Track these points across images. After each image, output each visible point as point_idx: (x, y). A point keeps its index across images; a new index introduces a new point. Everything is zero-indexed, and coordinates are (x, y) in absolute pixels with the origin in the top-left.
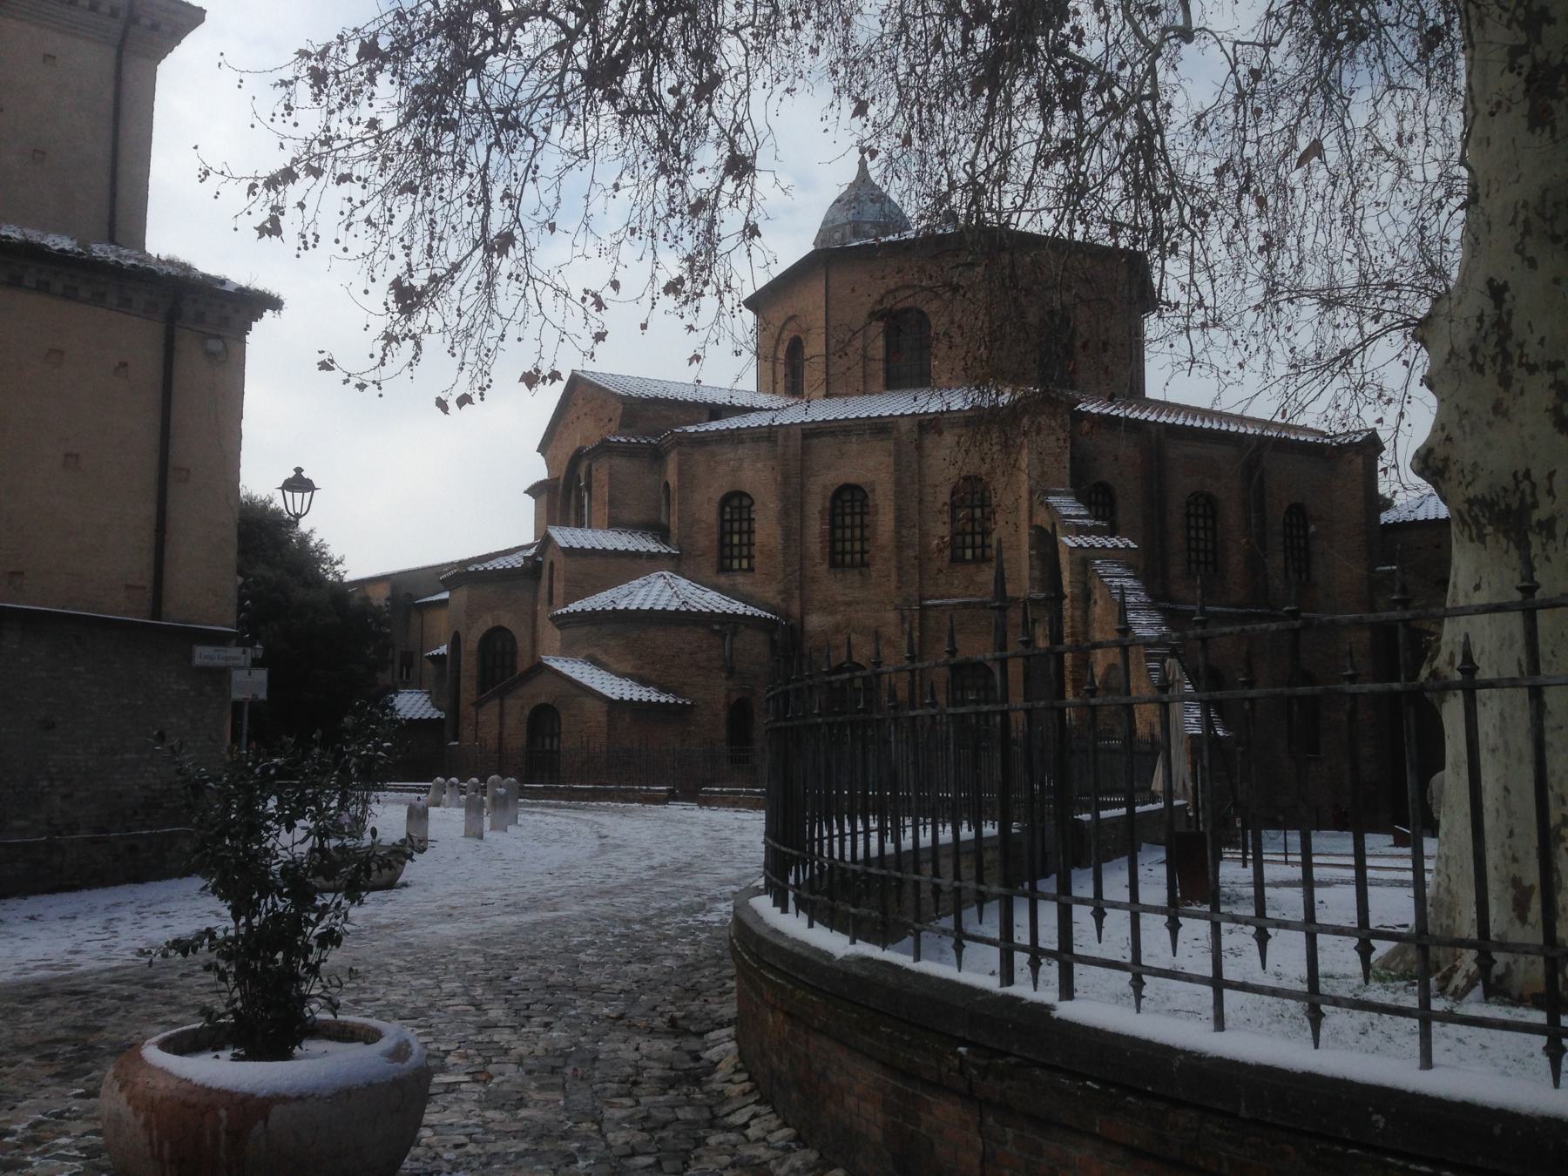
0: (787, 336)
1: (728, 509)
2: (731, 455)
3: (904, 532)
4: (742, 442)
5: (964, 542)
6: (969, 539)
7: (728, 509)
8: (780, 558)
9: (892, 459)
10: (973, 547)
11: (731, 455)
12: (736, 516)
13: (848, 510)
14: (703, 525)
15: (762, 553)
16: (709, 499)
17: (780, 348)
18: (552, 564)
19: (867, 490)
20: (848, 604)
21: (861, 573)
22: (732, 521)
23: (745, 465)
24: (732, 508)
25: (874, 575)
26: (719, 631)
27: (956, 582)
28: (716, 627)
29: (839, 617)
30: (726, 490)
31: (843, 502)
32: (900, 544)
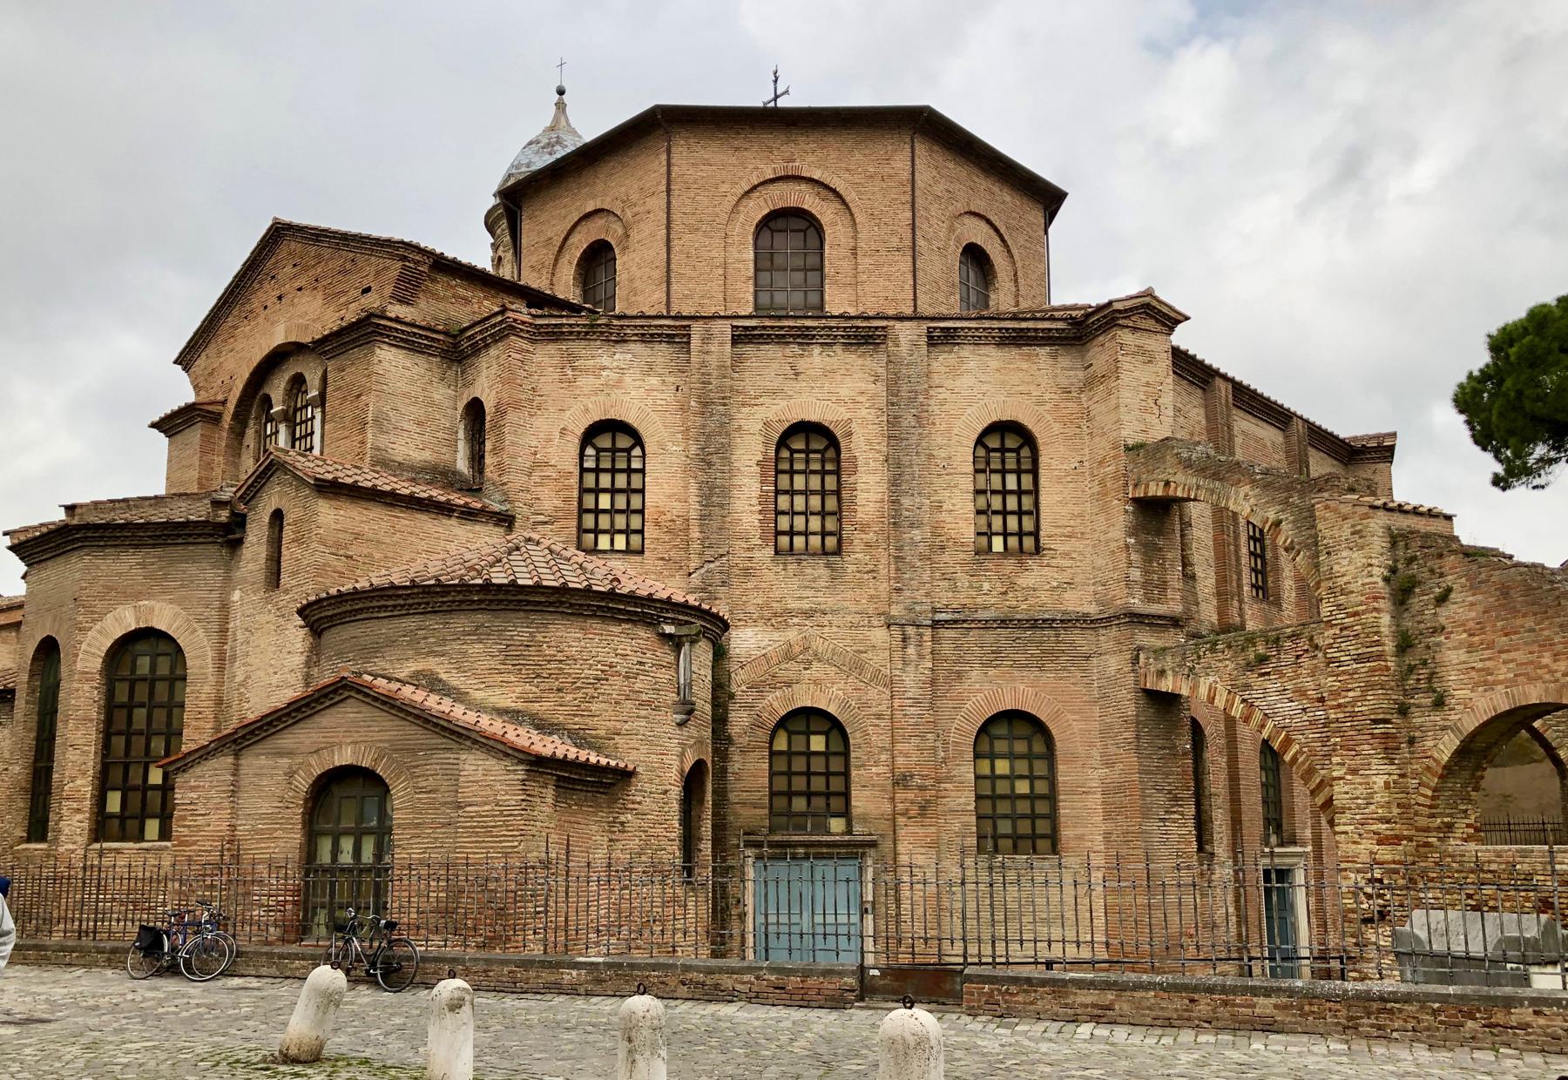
0: (580, 242)
1: (590, 451)
2: (605, 361)
3: (906, 501)
4: (623, 341)
5: (990, 525)
6: (997, 522)
7: (590, 451)
8: (695, 534)
9: (881, 388)
10: (1005, 534)
11: (605, 361)
12: (606, 464)
13: (798, 466)
14: (549, 472)
15: (657, 524)
16: (563, 431)
17: (564, 260)
18: (278, 516)
19: (838, 433)
20: (808, 614)
21: (828, 566)
22: (597, 471)
23: (627, 379)
24: (599, 450)
25: (851, 568)
26: (670, 636)
27: (986, 586)
28: (669, 629)
29: (792, 635)
30: (596, 417)
31: (793, 452)
32: (896, 520)
